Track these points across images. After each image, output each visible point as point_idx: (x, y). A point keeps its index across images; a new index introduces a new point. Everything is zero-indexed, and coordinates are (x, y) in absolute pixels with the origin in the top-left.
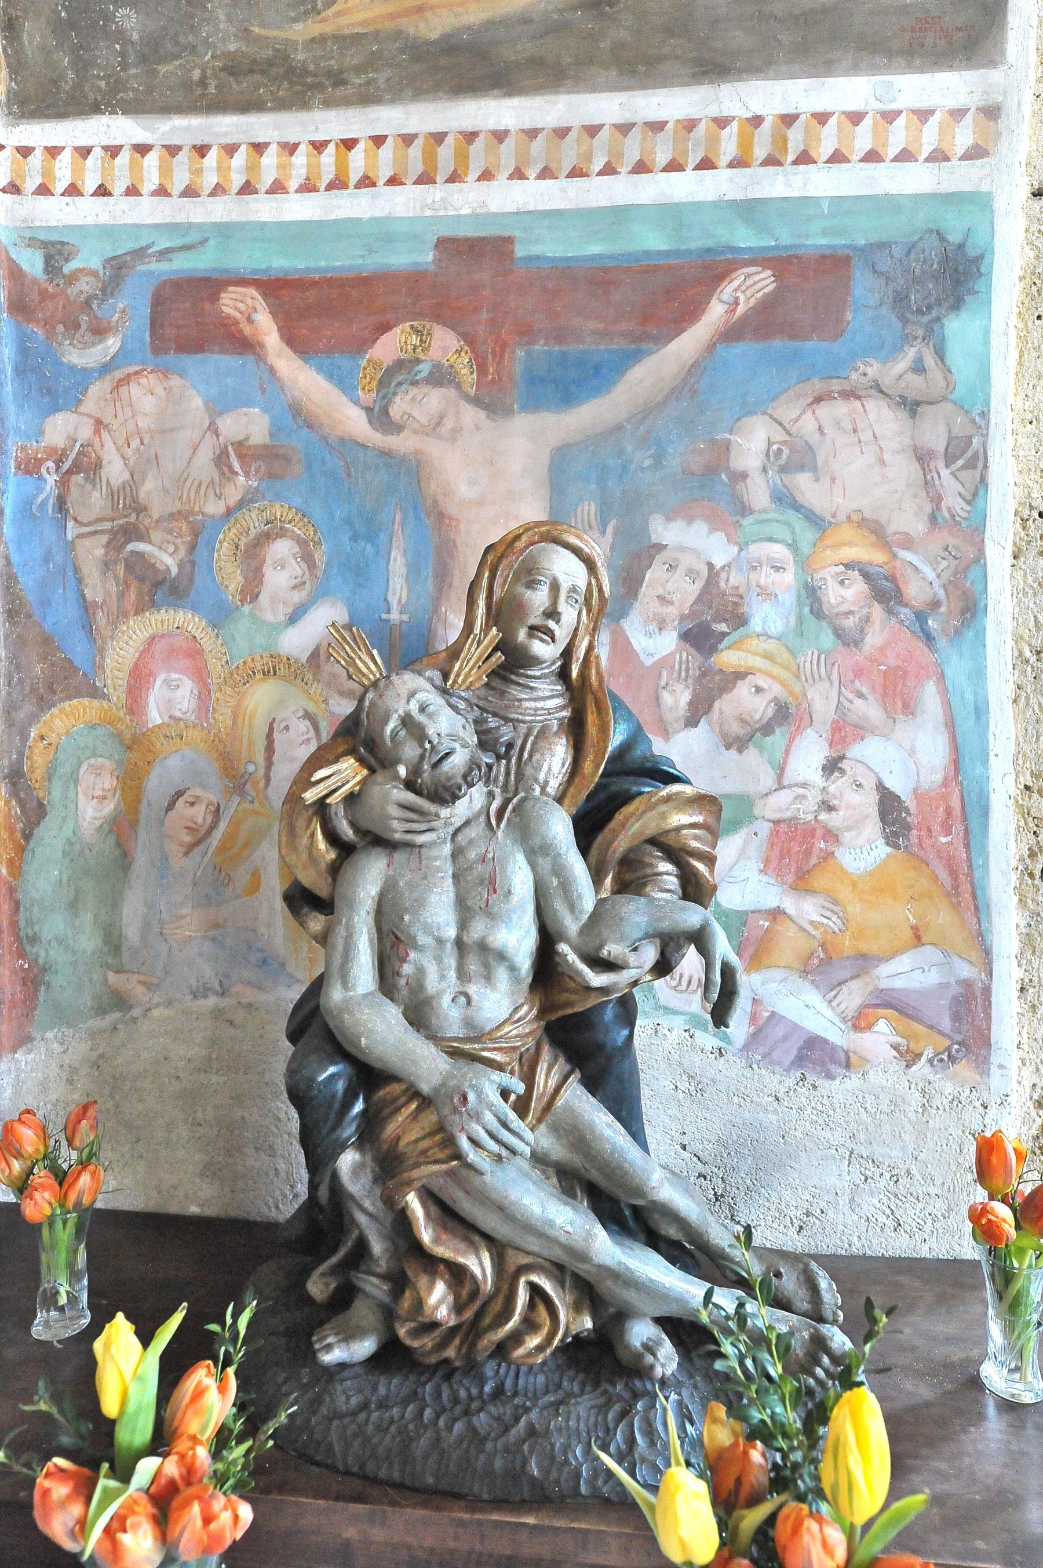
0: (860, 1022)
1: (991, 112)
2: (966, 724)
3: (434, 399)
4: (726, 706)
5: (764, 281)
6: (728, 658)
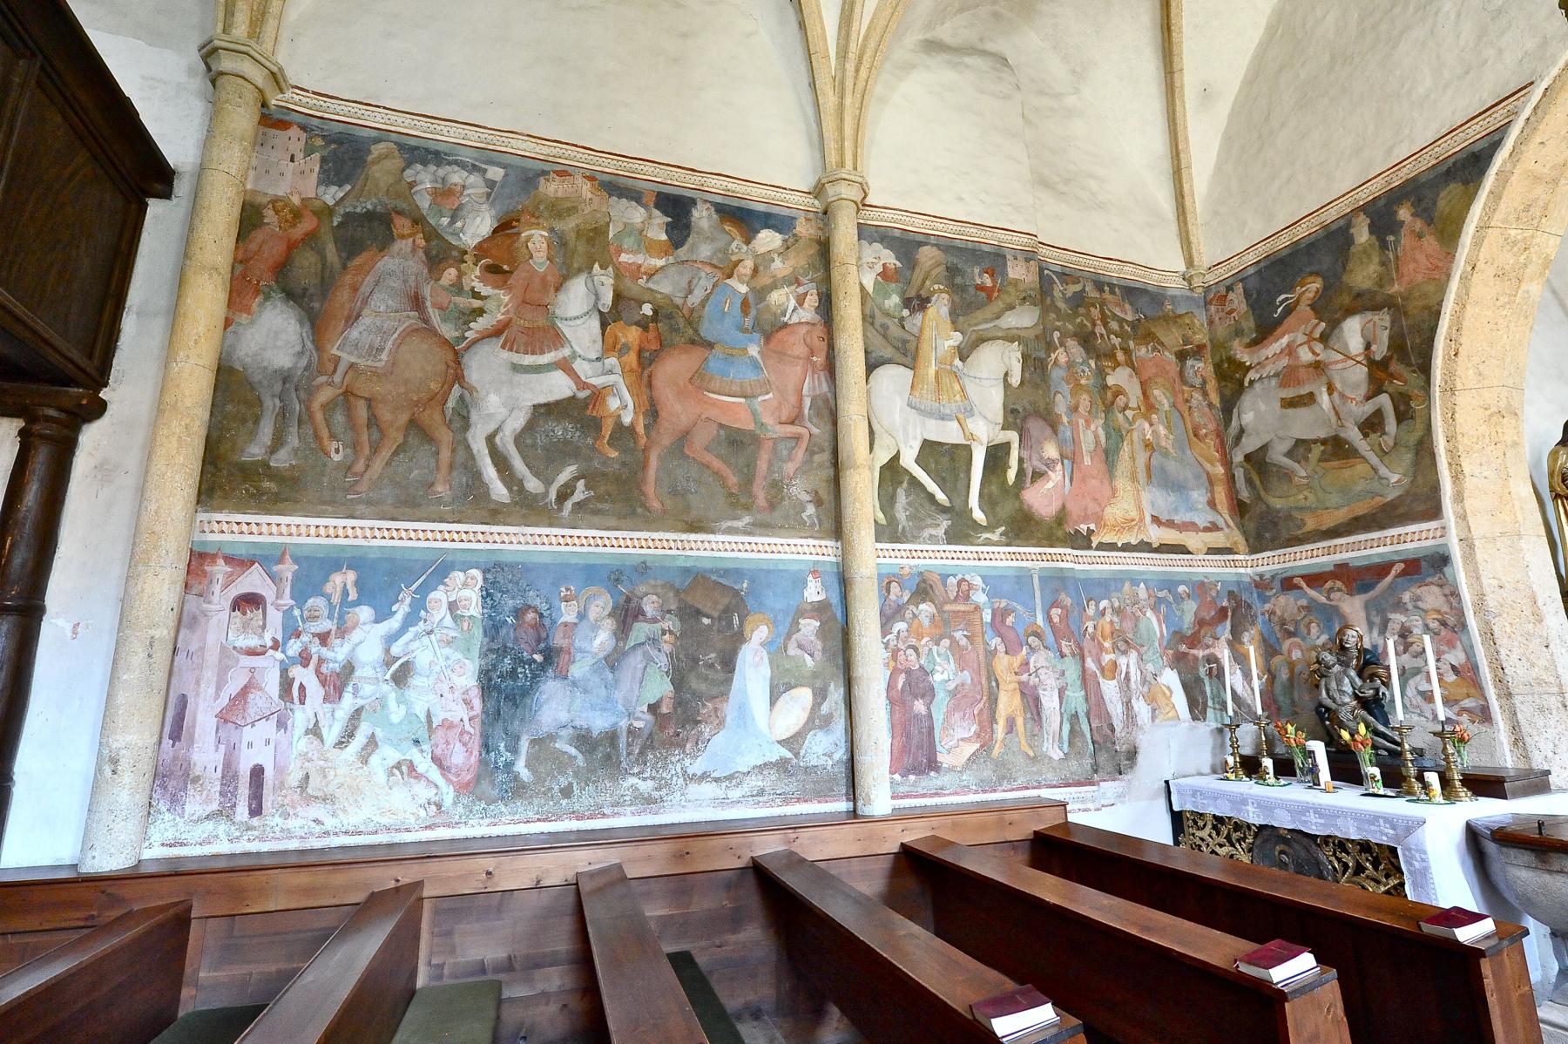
0: (1459, 714)
1: (1444, 528)
2: (1468, 650)
3: (1339, 594)
4: (1411, 649)
5: (1402, 565)
6: (1410, 640)
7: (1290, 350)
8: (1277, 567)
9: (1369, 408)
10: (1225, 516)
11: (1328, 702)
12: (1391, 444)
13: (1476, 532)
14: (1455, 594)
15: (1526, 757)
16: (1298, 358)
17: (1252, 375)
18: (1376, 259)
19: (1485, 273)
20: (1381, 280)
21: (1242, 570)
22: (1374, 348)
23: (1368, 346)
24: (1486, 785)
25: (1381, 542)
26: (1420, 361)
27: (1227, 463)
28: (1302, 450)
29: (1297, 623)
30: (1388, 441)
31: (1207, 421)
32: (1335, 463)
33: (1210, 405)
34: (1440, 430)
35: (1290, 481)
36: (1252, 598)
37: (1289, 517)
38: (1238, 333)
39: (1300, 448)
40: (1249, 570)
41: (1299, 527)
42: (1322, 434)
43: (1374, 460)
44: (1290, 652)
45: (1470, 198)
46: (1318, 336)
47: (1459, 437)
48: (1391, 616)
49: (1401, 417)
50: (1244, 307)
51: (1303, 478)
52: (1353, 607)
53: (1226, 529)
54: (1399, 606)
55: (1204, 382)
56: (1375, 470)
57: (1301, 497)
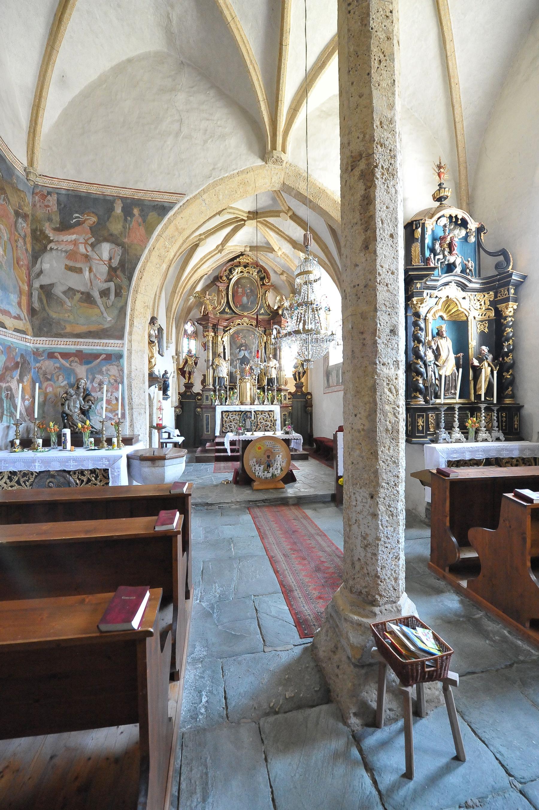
0: (114, 416)
1: (123, 344)
3: (76, 364)
5: (105, 356)
7: (75, 243)
8: (47, 346)
9: (105, 286)
10: (24, 314)
11: (68, 411)
12: (111, 304)
13: (134, 348)
14: (122, 370)
15: (133, 431)
16: (78, 248)
17: (52, 245)
18: (121, 224)
19: (155, 254)
20: (122, 233)
21: (28, 344)
22: (113, 261)
23: (110, 259)
24: (128, 441)
25: (98, 344)
26: (129, 275)
27: (30, 286)
28: (71, 293)
29: (52, 375)
30: (110, 303)
31: (25, 260)
32: (86, 305)
33: (26, 250)
34: (130, 305)
35: (62, 306)
36: (31, 359)
37: (58, 323)
38: (50, 220)
39: (70, 292)
40: (31, 345)
41: (63, 329)
42: (82, 289)
43: (103, 309)
44: (46, 388)
45: (159, 223)
46: (90, 243)
47: (135, 310)
48: (97, 376)
49: (118, 294)
50: (55, 208)
51: (69, 307)
52: (81, 370)
53: (24, 321)
54: (101, 372)
55: (25, 236)
56: (102, 314)
57: (67, 315)
